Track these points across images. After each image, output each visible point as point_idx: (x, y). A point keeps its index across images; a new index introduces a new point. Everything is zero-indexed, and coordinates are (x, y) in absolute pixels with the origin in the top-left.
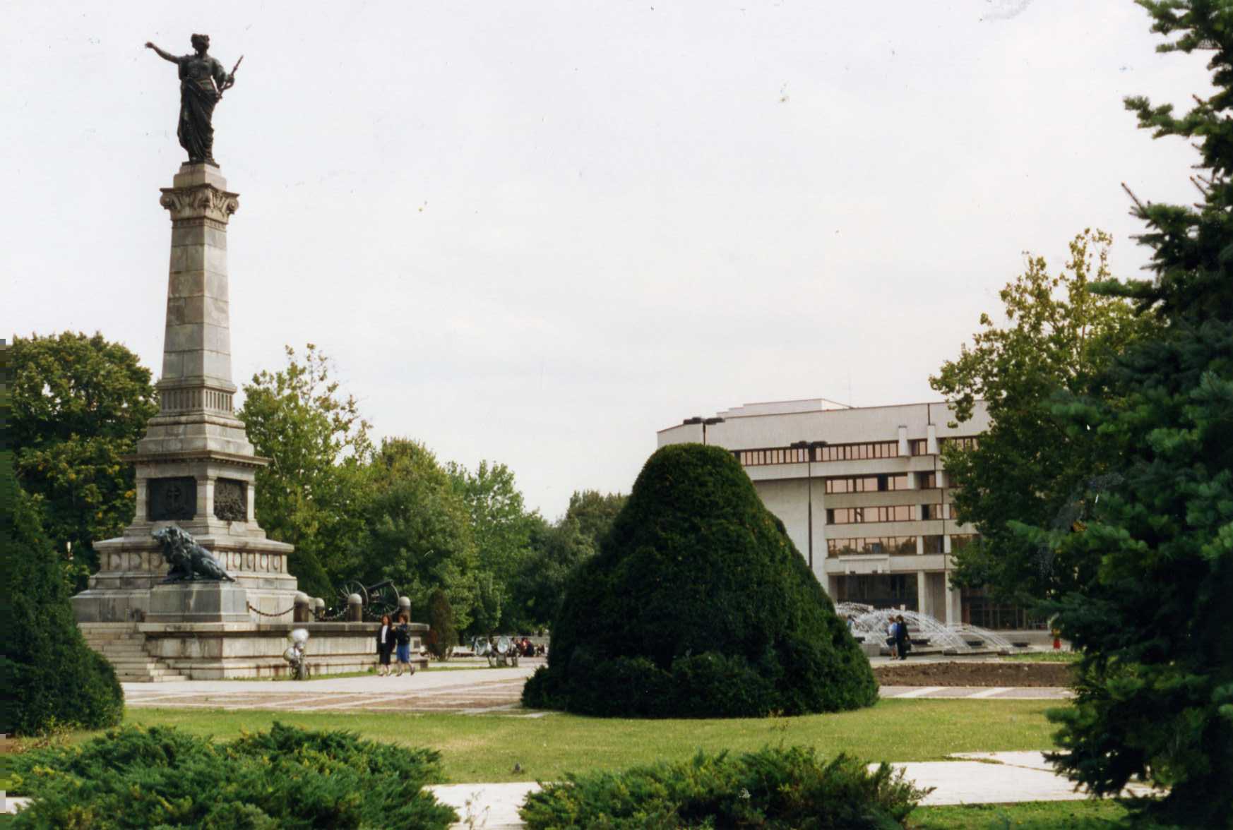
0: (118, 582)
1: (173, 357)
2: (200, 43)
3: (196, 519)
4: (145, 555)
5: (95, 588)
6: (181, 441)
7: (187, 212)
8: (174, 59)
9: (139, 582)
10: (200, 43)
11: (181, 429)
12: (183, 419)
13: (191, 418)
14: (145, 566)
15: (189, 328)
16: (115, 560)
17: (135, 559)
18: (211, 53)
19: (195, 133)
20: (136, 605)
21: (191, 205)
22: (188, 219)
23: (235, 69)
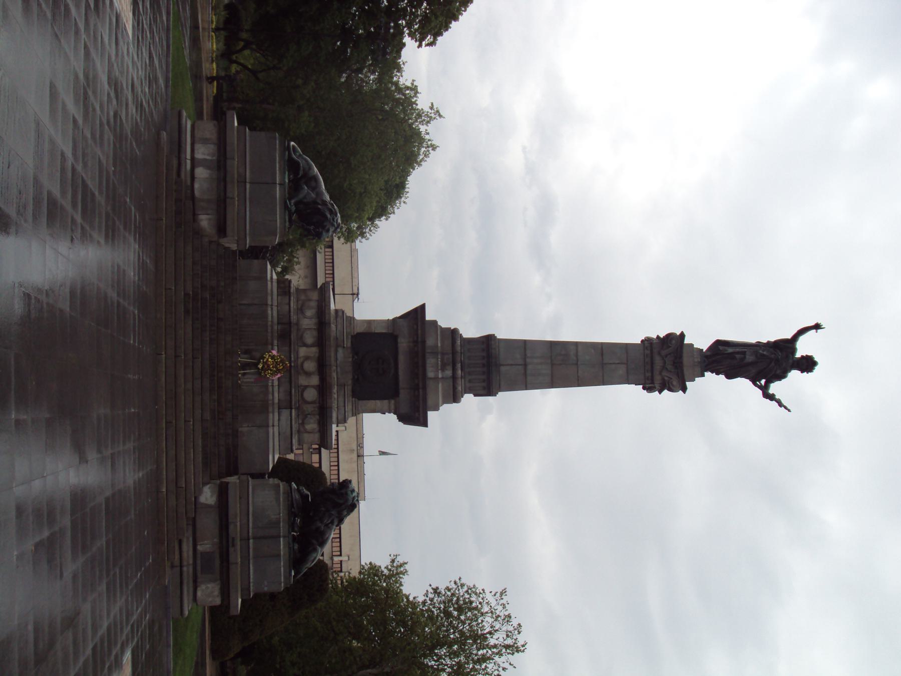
2: (808, 364)
10: (808, 364)
11: (449, 373)
14: (303, 351)
17: (309, 338)
18: (794, 374)
23: (780, 404)
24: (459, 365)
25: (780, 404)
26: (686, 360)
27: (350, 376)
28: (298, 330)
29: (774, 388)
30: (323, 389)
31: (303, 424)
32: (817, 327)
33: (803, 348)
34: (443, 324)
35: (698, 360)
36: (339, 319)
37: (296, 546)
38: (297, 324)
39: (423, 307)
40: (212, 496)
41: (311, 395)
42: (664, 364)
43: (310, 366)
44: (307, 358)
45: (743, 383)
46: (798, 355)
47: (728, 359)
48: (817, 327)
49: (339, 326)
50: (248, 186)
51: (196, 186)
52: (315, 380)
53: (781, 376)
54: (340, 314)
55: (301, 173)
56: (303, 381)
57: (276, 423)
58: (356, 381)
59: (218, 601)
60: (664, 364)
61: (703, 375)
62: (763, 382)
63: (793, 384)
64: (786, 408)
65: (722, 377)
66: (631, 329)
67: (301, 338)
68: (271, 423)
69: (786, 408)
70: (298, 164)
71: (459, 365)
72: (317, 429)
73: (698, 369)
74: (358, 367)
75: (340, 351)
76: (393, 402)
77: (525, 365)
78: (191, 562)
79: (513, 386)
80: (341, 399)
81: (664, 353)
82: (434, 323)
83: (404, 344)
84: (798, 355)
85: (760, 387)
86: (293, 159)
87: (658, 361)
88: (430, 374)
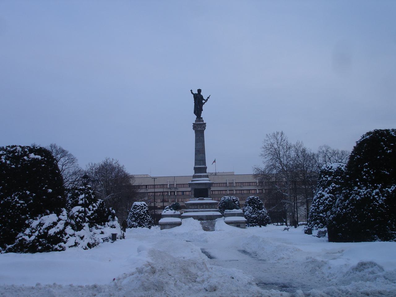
2: (199, 91)
7: (199, 129)
10: (199, 91)
21: (201, 127)
22: (200, 130)
23: (208, 98)
29: (205, 98)
33: (196, 92)
42: (199, 128)
46: (197, 93)
47: (198, 110)
53: (202, 97)
60: (199, 128)
61: (202, 118)
62: (203, 101)
63: (204, 95)
66: (192, 134)
77: (200, 160)
83: (197, 187)
84: (197, 93)
85: (205, 103)
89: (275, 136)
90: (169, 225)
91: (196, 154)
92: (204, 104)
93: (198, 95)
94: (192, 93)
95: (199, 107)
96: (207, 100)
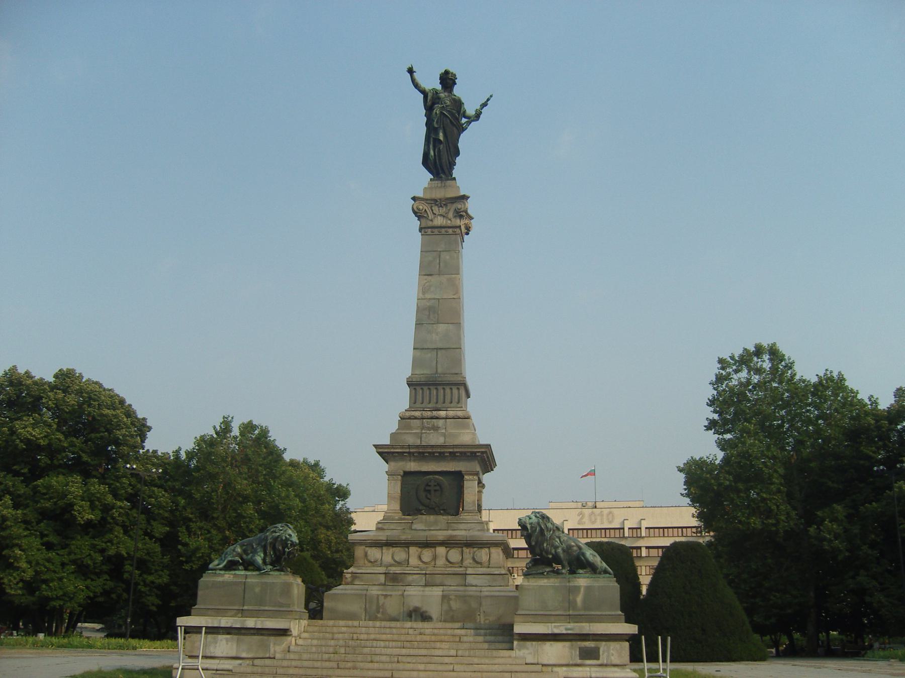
0: (382, 578)
1: (418, 353)
2: (448, 80)
3: (464, 516)
4: (413, 550)
5: (352, 583)
6: (444, 435)
8: (423, 92)
9: (410, 578)
10: (448, 80)
11: (440, 423)
12: (443, 413)
13: (451, 413)
14: (414, 561)
15: (442, 328)
16: (374, 553)
17: (400, 554)
18: (457, 91)
19: (440, 157)
20: (415, 603)
23: (484, 105)
24: (435, 413)
25: (484, 105)
26: (439, 194)
27: (441, 518)
28: (391, 565)
29: (470, 110)
30: (448, 543)
31: (481, 563)
32: (411, 71)
33: (432, 83)
34: (394, 427)
35: (437, 183)
36: (385, 527)
37: (581, 571)
38: (387, 566)
39: (376, 446)
40: (527, 649)
41: (454, 555)
43: (427, 554)
44: (420, 558)
45: (465, 141)
48: (411, 71)
49: (392, 527)
50: (245, 608)
51: (244, 655)
52: (441, 550)
53: (458, 104)
54: (380, 525)
55: (237, 558)
56: (441, 562)
57: (478, 589)
58: (446, 512)
59: (627, 644)
62: (464, 120)
63: (467, 93)
64: (488, 100)
65: (458, 160)
67: (399, 564)
68: (478, 594)
69: (488, 100)
70: (230, 561)
71: (435, 413)
72: (487, 550)
73: (449, 183)
74: (433, 510)
75: (414, 526)
76: (466, 477)
78: (588, 669)
79: (458, 361)
80: (462, 526)
81: (431, 216)
82: (393, 435)
83: (413, 466)
84: (439, 87)
85: (469, 123)
86: (225, 566)
87: (439, 221)
88: (441, 441)
89: (745, 360)
90: (228, 634)
91: (419, 324)
92: (464, 130)
93: (442, 95)
94: (416, 85)
95: (441, 136)
96: (478, 116)
